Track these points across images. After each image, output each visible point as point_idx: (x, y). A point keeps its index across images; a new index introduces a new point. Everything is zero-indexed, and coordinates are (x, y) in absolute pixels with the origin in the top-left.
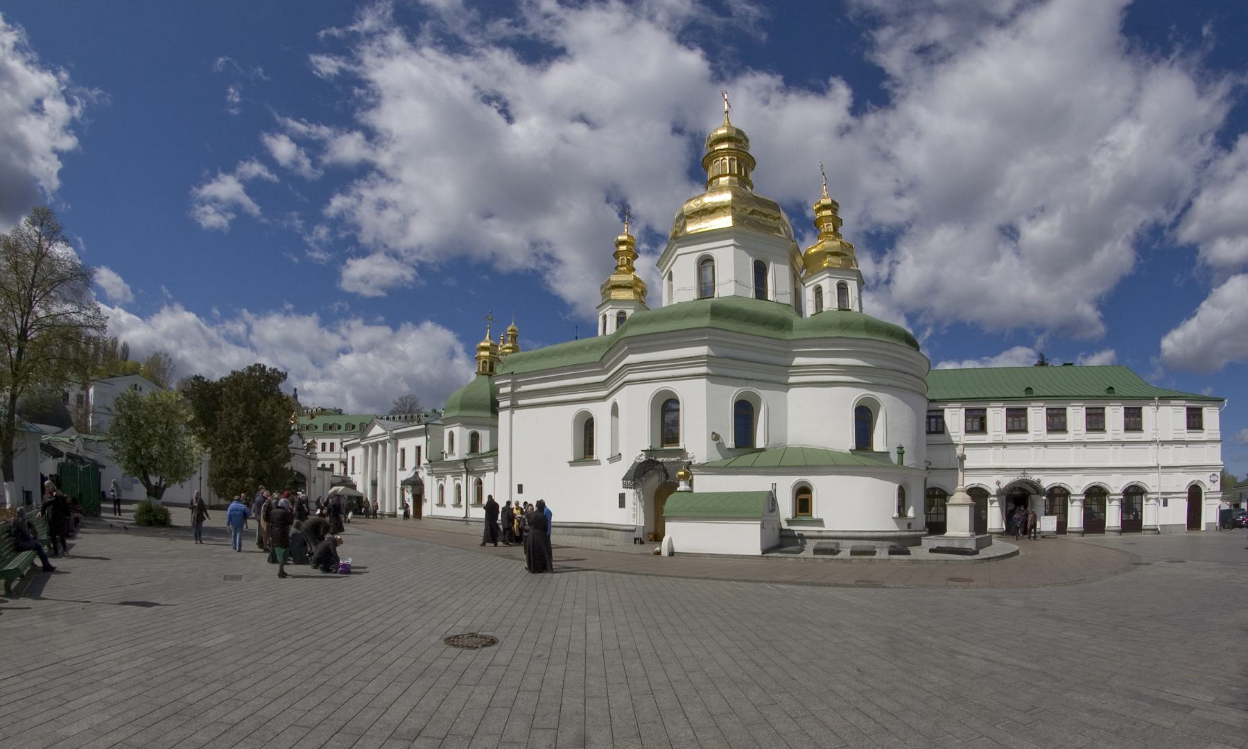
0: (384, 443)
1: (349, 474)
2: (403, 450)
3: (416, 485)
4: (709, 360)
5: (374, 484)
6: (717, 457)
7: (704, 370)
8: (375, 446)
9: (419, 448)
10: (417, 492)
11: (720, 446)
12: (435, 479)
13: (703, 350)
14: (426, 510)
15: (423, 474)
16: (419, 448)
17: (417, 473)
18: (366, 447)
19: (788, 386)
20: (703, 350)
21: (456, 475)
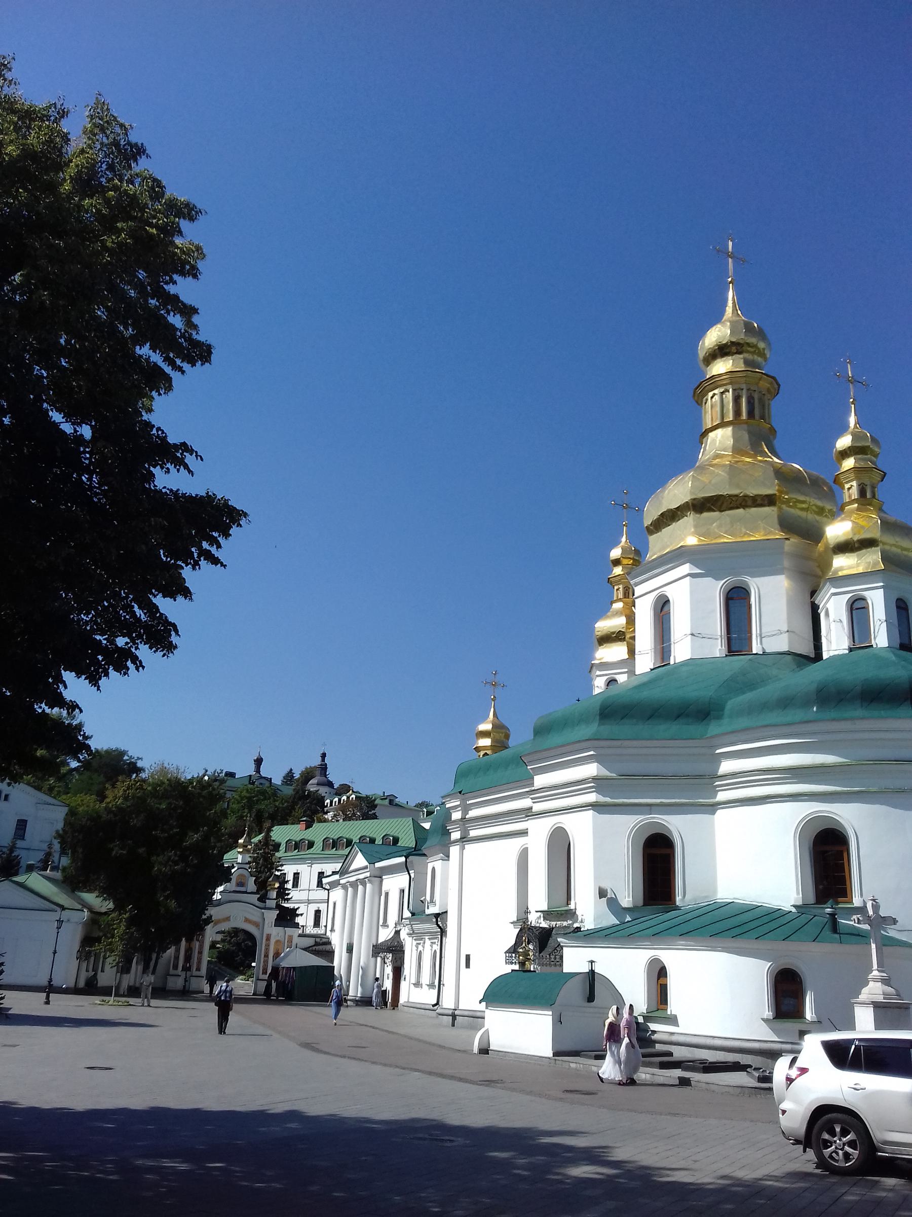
0: (363, 882)
1: (328, 933)
2: (387, 894)
3: (394, 949)
4: (598, 783)
5: (350, 949)
6: (613, 920)
7: (592, 797)
8: (354, 885)
9: (403, 891)
10: (399, 964)
11: (613, 904)
12: (415, 943)
13: (591, 770)
14: (408, 993)
15: (403, 935)
16: (403, 891)
17: (397, 933)
18: (345, 887)
19: (713, 808)
20: (591, 770)
21: (432, 935)
